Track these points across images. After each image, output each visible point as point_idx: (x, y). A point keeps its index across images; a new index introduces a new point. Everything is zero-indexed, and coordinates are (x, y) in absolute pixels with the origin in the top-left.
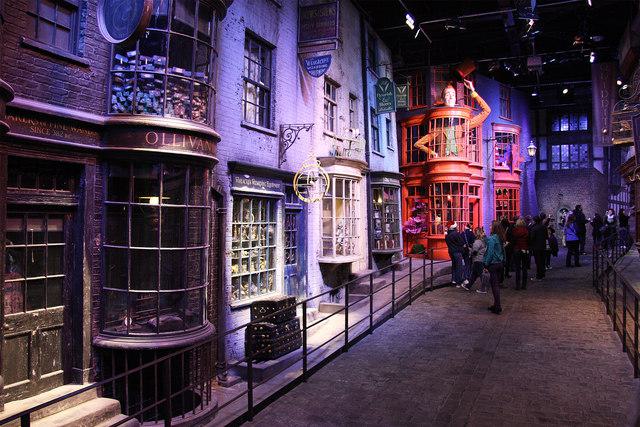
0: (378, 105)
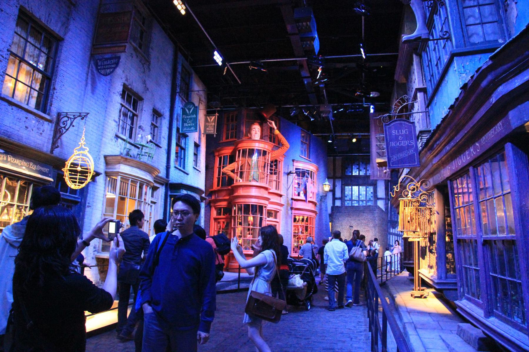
0: (183, 125)
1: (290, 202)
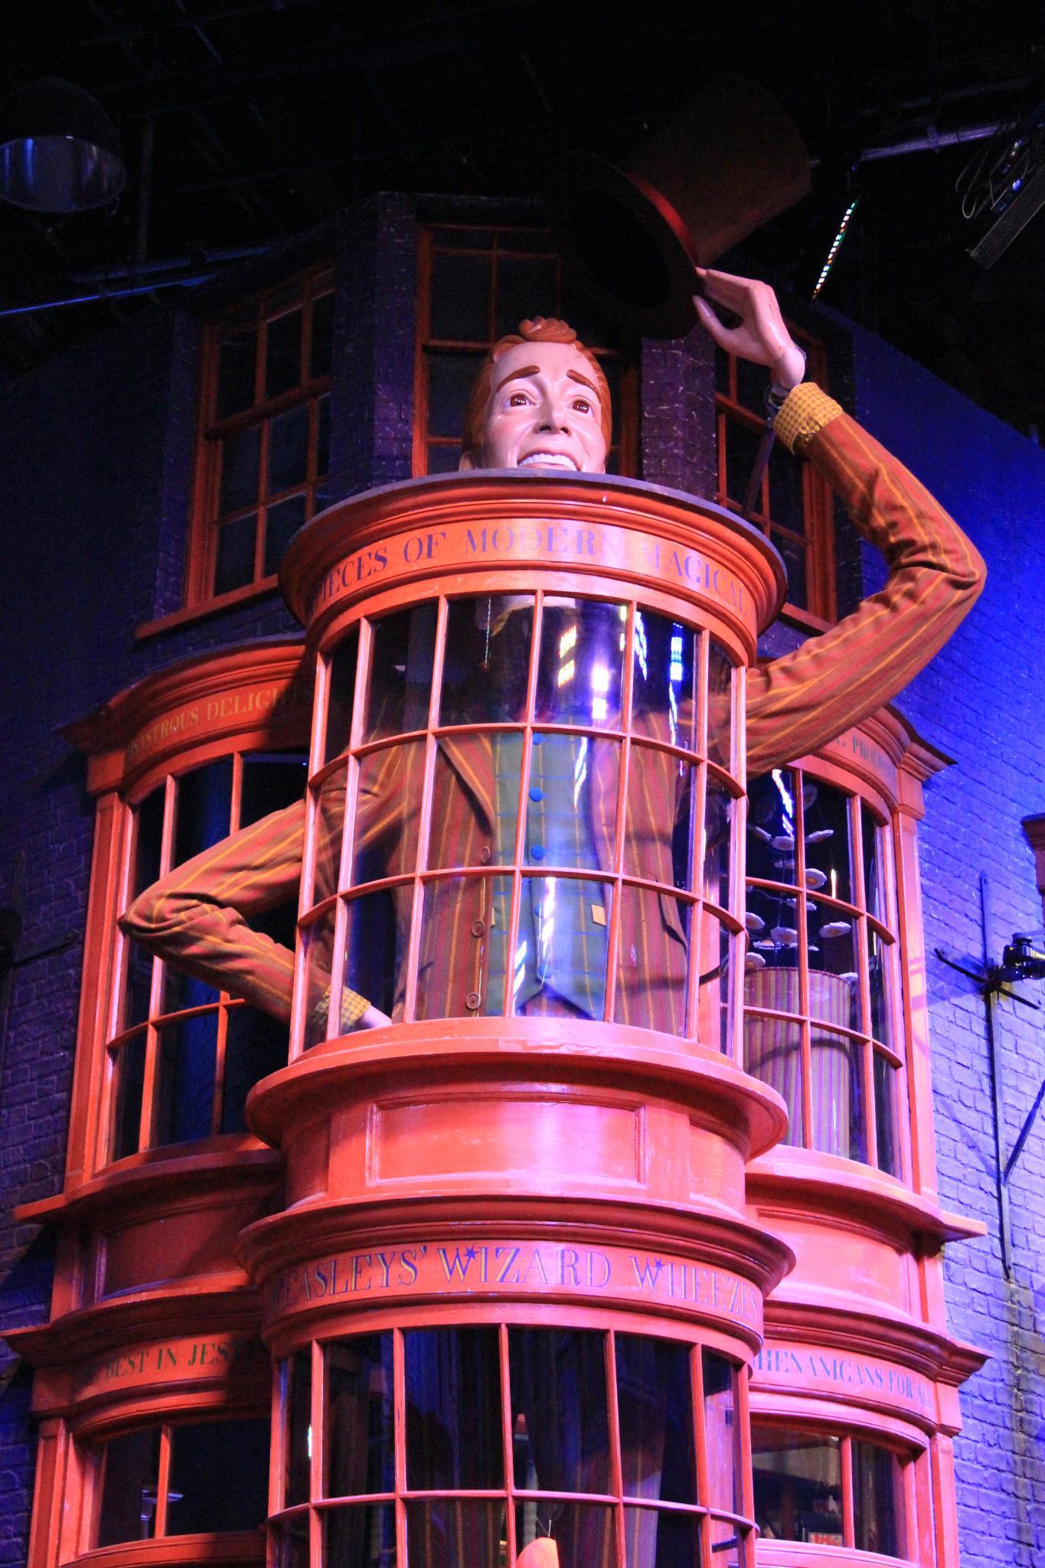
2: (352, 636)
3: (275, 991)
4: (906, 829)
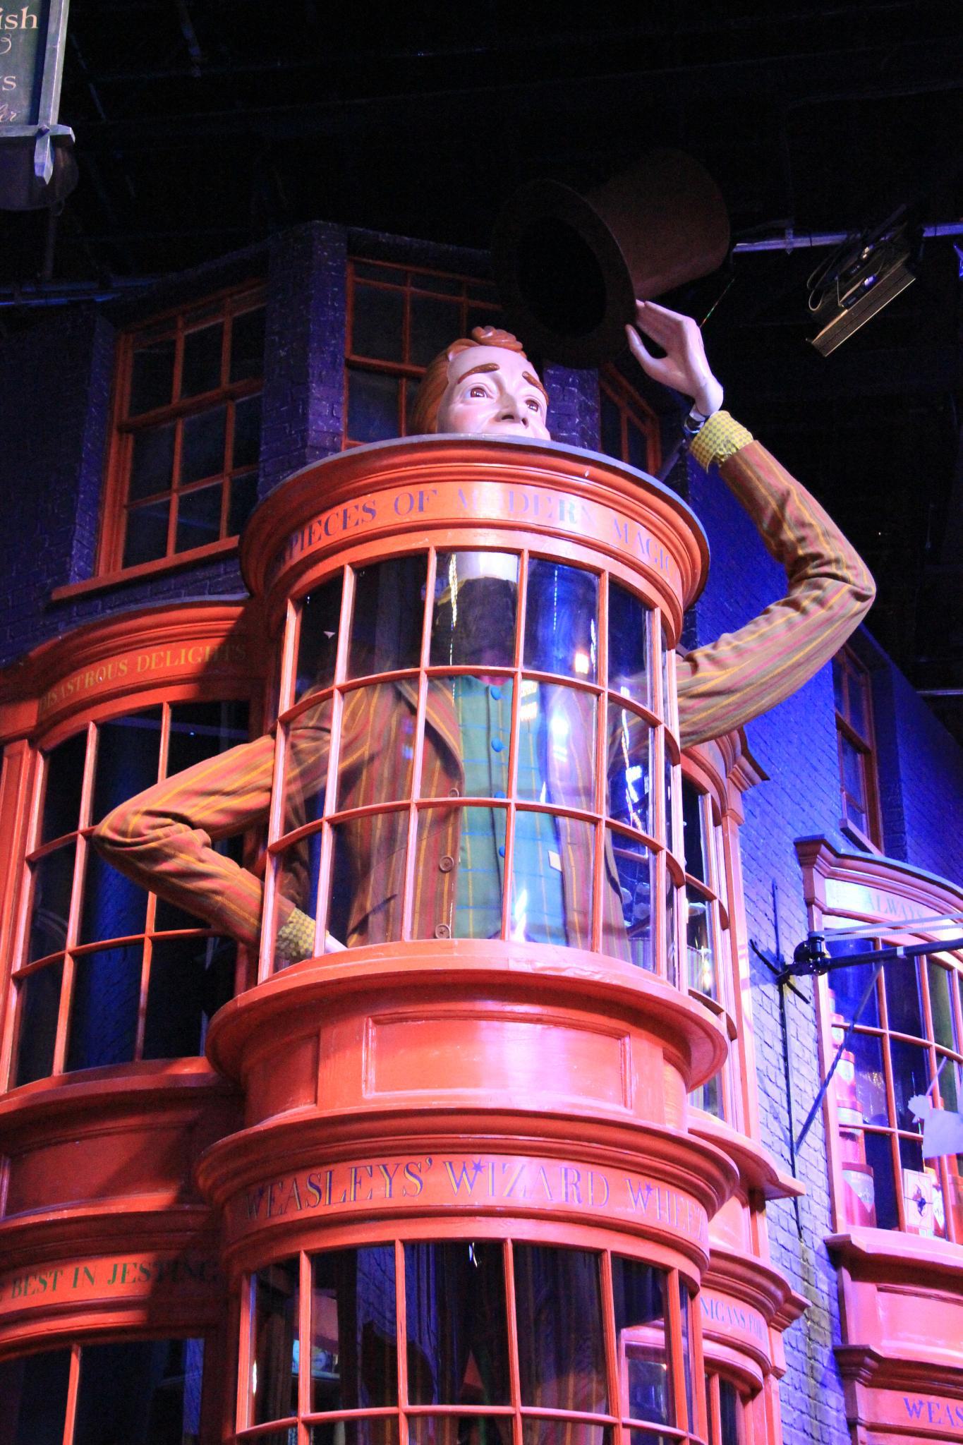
1: (823, 1281)
2: (336, 580)
3: (241, 913)
4: (733, 832)
